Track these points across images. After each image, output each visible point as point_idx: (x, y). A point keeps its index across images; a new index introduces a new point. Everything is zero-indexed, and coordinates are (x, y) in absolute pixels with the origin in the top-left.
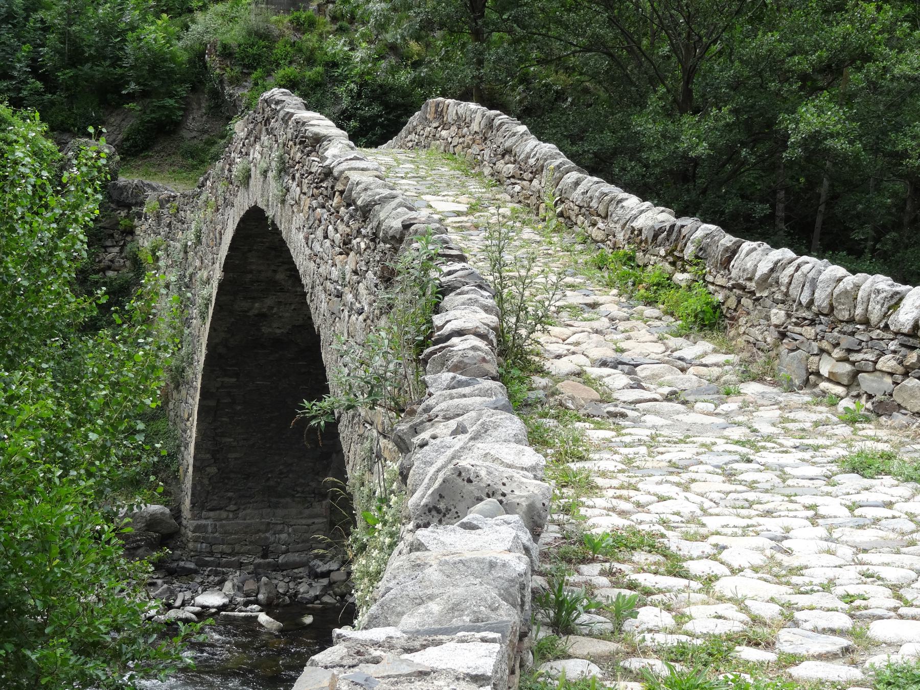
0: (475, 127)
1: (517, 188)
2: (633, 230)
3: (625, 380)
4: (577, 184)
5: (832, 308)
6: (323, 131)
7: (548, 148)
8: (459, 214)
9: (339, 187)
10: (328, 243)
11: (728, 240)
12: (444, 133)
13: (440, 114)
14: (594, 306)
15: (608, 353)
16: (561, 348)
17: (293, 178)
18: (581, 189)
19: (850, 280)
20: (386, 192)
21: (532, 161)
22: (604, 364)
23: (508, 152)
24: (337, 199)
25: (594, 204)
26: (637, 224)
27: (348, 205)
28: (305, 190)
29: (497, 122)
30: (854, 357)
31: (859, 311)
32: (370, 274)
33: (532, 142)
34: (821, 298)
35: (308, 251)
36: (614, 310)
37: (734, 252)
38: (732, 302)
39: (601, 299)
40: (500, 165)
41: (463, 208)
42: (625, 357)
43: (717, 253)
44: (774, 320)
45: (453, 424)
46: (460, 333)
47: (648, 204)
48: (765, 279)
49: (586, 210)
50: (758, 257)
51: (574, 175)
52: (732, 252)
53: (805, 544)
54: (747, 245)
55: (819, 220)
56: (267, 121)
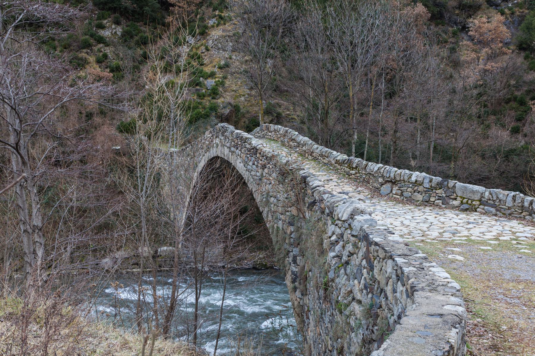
1: (298, 149)
2: (337, 160)
4: (317, 148)
5: (395, 178)
12: (270, 134)
14: (331, 180)
15: (341, 191)
19: (399, 171)
21: (302, 142)
22: (340, 193)
24: (258, 155)
26: (338, 158)
27: (263, 156)
28: (243, 152)
31: (402, 178)
33: (301, 137)
34: (392, 175)
35: (245, 169)
38: (367, 177)
39: (332, 178)
40: (291, 143)
42: (345, 191)
43: (363, 166)
44: (380, 181)
45: (342, 202)
46: (318, 186)
47: (339, 153)
48: (376, 171)
49: (322, 155)
50: (374, 167)
51: (316, 146)
54: (370, 163)
55: (365, 152)
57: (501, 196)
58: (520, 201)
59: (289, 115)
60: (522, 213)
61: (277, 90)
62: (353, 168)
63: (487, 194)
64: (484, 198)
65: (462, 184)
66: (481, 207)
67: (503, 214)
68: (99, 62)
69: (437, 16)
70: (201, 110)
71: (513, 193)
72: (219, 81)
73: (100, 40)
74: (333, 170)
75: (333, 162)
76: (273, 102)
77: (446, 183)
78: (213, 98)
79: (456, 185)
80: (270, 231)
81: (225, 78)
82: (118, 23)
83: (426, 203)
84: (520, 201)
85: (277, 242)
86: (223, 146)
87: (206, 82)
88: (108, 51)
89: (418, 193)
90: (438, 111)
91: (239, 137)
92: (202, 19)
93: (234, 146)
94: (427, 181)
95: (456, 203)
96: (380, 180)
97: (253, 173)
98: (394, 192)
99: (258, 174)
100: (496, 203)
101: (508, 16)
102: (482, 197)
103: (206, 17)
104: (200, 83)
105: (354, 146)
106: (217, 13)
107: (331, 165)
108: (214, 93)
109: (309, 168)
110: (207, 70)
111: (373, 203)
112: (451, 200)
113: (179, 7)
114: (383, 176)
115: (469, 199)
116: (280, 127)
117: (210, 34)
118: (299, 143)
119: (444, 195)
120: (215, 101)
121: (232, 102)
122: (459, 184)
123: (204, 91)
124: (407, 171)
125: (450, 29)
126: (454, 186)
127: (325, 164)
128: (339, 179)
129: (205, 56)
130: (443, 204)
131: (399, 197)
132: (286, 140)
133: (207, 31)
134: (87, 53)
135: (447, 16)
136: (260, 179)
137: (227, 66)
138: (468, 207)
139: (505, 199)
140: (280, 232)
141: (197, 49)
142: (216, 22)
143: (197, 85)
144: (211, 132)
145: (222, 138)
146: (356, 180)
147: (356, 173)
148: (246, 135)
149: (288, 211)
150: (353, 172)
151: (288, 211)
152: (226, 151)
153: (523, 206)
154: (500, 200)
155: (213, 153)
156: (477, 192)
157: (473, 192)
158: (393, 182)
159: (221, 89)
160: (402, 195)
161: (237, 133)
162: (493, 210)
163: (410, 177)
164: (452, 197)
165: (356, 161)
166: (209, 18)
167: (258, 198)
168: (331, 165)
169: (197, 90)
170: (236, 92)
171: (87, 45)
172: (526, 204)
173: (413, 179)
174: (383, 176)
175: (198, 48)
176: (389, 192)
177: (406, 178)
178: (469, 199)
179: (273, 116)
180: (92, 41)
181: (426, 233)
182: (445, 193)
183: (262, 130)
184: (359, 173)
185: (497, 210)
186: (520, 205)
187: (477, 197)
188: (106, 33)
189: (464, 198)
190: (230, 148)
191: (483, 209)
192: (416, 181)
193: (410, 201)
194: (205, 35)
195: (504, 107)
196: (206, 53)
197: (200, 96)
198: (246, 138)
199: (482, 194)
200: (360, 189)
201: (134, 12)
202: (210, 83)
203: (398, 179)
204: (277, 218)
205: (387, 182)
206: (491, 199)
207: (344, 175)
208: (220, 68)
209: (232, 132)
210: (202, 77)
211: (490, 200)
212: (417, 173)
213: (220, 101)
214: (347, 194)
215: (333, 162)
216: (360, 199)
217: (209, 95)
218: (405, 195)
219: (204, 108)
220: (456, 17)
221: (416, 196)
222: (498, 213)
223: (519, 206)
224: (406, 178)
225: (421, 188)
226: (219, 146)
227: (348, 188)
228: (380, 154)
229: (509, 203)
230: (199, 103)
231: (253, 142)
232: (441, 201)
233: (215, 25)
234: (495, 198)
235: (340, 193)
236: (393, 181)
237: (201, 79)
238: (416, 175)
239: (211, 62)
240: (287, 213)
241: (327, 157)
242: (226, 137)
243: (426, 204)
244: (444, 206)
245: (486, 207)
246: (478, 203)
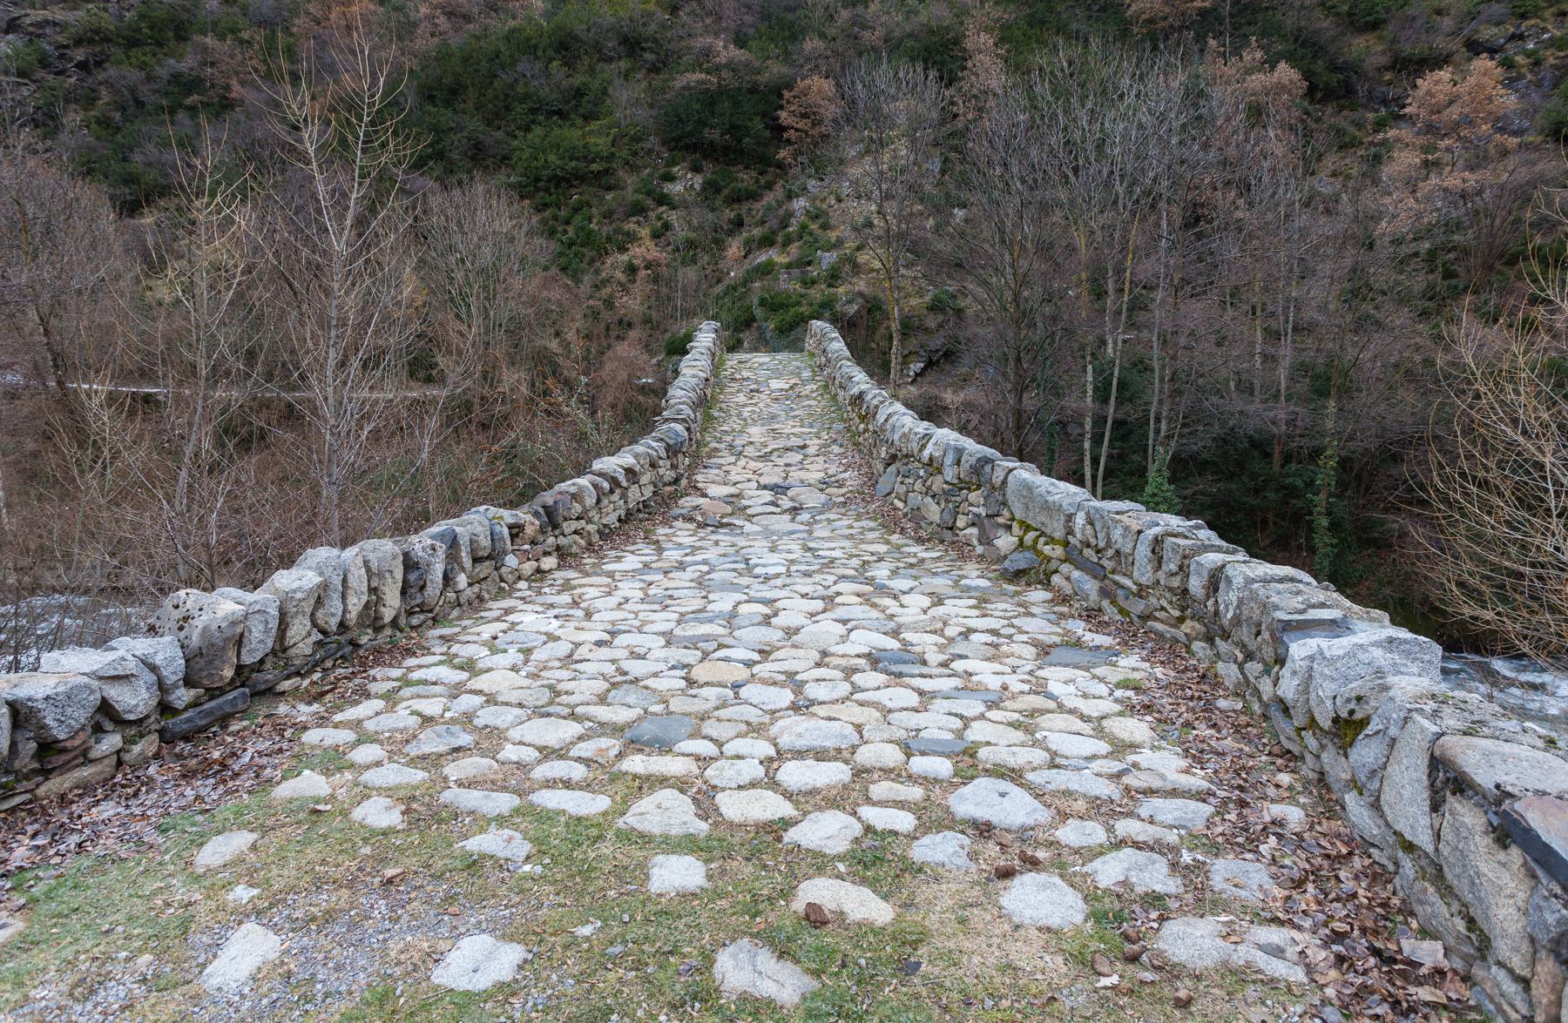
60: (1181, 620)
63: (1080, 519)
66: (1065, 568)
67: (1122, 611)
68: (656, 235)
69: (1331, 86)
73: (663, 200)
79: (1010, 478)
82: (696, 169)
84: (1173, 567)
88: (673, 217)
90: (1319, 295)
100: (1105, 562)
102: (1070, 532)
110: (833, 235)
113: (797, 130)
115: (1043, 534)
119: (982, 511)
120: (832, 290)
125: (1370, 116)
134: (638, 223)
135: (1362, 90)
141: (823, 200)
153: (1185, 591)
163: (924, 446)
164: (1000, 520)
171: (638, 210)
172: (1196, 585)
180: (649, 202)
185: (1104, 593)
186: (1176, 582)
188: (675, 189)
191: (1068, 579)
192: (931, 459)
201: (727, 149)
206: (1093, 541)
211: (1088, 546)
220: (1384, 89)
223: (1171, 589)
224: (915, 446)
225: (937, 484)
229: (1143, 572)
234: (1102, 544)
246: (1060, 551)
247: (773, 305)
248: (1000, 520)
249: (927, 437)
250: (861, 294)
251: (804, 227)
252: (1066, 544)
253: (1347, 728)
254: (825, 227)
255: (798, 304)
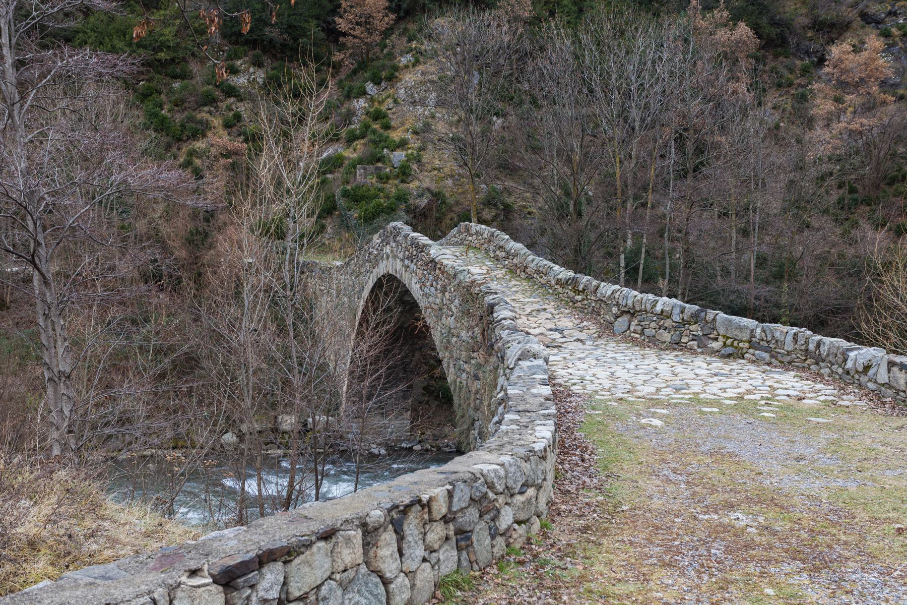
0: (485, 236)
3: (560, 335)
6: (426, 242)
7: (519, 245)
8: (482, 274)
9: (438, 266)
10: (433, 289)
11: (595, 282)
12: (470, 238)
13: (467, 230)
14: (545, 309)
15: (553, 327)
16: (536, 325)
17: (412, 261)
18: (534, 263)
20: (461, 268)
22: (551, 330)
23: (501, 247)
24: (437, 271)
25: (541, 269)
26: (560, 277)
29: (496, 234)
30: (642, 323)
32: (457, 301)
33: (512, 243)
34: (630, 302)
35: (422, 293)
36: (552, 310)
37: (598, 287)
39: (547, 306)
40: (498, 252)
41: (485, 272)
42: (559, 328)
43: (592, 288)
44: (614, 312)
46: (505, 319)
49: (538, 272)
50: (607, 289)
51: (531, 257)
52: (597, 287)
53: (620, 372)
54: (603, 284)
55: (641, 267)
56: (395, 237)
57: (777, 334)
58: (802, 342)
59: (525, 207)
60: (806, 360)
61: (507, 168)
62: (580, 291)
63: (759, 331)
64: (755, 337)
65: (726, 316)
66: (751, 351)
67: (780, 362)
68: (228, 126)
70: (382, 201)
71: (796, 329)
72: (412, 154)
73: (231, 92)
74: (552, 294)
75: (553, 282)
76: (499, 186)
77: (703, 314)
78: (403, 181)
80: (452, 389)
81: (422, 149)
82: (258, 64)
83: (676, 345)
84: (802, 342)
85: (460, 405)
86: (395, 257)
87: (392, 156)
88: (243, 108)
89: (665, 329)
90: (771, 201)
91: (415, 244)
92: (391, 56)
93: (408, 258)
94: (677, 311)
95: (716, 345)
96: (615, 310)
97: (431, 299)
98: (632, 329)
99: (438, 301)
100: (771, 346)
101: (897, 39)
103: (397, 51)
104: (384, 157)
105: (622, 256)
106: (414, 45)
107: (551, 287)
108: (404, 173)
109: (517, 292)
110: (396, 136)
111: (597, 345)
112: (710, 341)
113: (355, 37)
114: (618, 305)
115: (735, 339)
116: (483, 227)
117: (401, 79)
118: (508, 253)
119: (701, 333)
120: (404, 186)
121: (433, 187)
122: (722, 315)
123: (388, 170)
124: (651, 296)
125: (798, 63)
126: (714, 320)
127: (543, 286)
128: (558, 308)
129: (394, 114)
130: (699, 347)
131: (638, 336)
132: (491, 248)
133: (397, 74)
134: (210, 112)
135: (793, 41)
136: (440, 309)
137: (427, 128)
138: (732, 353)
139: (782, 339)
140: (463, 390)
141: (381, 102)
142: (413, 60)
143: (379, 160)
144: (380, 236)
145: (394, 245)
146: (582, 310)
147: (583, 299)
148: (424, 240)
149: (473, 358)
150: (579, 298)
151: (473, 358)
152: (399, 264)
153: (807, 350)
154: (777, 341)
155: (382, 268)
156: (746, 327)
157: (740, 328)
158: (632, 313)
159: (415, 167)
160: (642, 333)
161: (412, 238)
162: (766, 356)
163: (655, 306)
164: (711, 336)
165: (584, 280)
166: (401, 55)
167: (437, 338)
168: (551, 287)
169: (377, 168)
170: (439, 172)
171: (209, 101)
172: (812, 347)
173: (658, 308)
174: (618, 305)
175: (383, 101)
176: (625, 328)
177: (649, 307)
178: (735, 339)
179: (498, 209)
180: (217, 93)
181: (638, 388)
182: (702, 330)
183: (459, 232)
184: (587, 299)
185: (772, 356)
186: (803, 348)
187: (746, 336)
188: (240, 81)
189: (728, 338)
190: (403, 260)
191: (753, 355)
192: (662, 311)
193: (653, 342)
194: (394, 80)
195: (885, 192)
196: (394, 110)
197: (381, 179)
198: (425, 246)
199: (752, 331)
200: (585, 323)
201: (284, 46)
202: (399, 156)
203: (638, 308)
204: (459, 369)
205: (623, 313)
207: (567, 303)
208: (416, 133)
209: (406, 236)
210: (387, 147)
212: (665, 299)
213: (413, 185)
214: (561, 331)
215: (553, 282)
216: (578, 340)
217: (397, 177)
218: (645, 333)
219: (387, 197)
220: (807, 43)
221: (661, 334)
222: (773, 360)
224: (649, 307)
225: (668, 323)
226: (390, 259)
227: (566, 323)
228: (668, 270)
229: (789, 346)
230: (379, 190)
231: (432, 252)
232: (695, 343)
233: (410, 64)
234: (769, 339)
235: (551, 330)
236: (632, 311)
237: (385, 150)
238: (664, 303)
239: (403, 124)
240: (473, 362)
241: (546, 275)
242: (398, 244)
243: (676, 346)
244: (699, 350)
245: (757, 352)
246: (747, 345)
247: (356, 197)
248: (711, 336)
249: (657, 301)
250: (428, 189)
251: (367, 127)
252: (750, 342)
253: (867, 368)
254: (387, 127)
255: (377, 196)
